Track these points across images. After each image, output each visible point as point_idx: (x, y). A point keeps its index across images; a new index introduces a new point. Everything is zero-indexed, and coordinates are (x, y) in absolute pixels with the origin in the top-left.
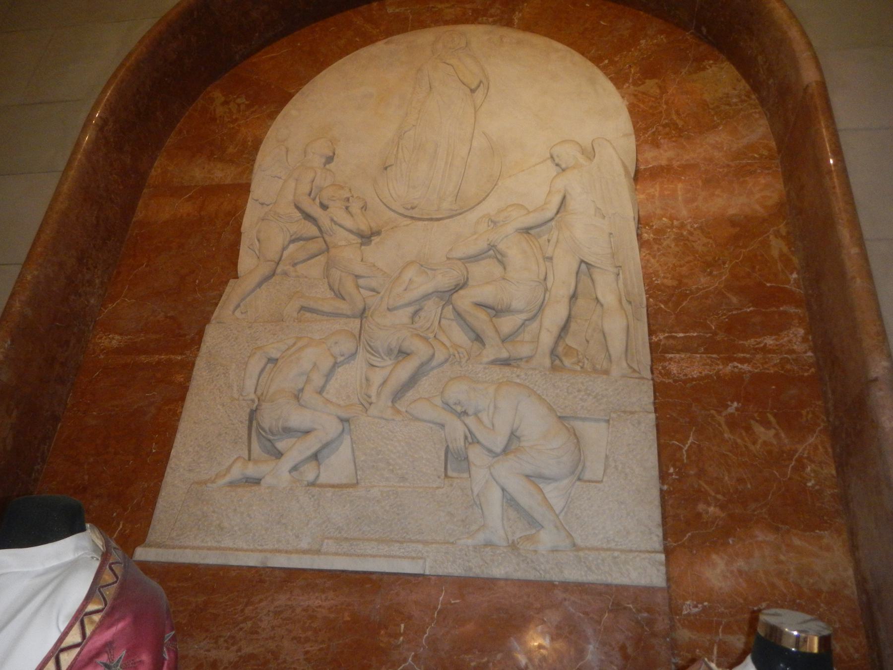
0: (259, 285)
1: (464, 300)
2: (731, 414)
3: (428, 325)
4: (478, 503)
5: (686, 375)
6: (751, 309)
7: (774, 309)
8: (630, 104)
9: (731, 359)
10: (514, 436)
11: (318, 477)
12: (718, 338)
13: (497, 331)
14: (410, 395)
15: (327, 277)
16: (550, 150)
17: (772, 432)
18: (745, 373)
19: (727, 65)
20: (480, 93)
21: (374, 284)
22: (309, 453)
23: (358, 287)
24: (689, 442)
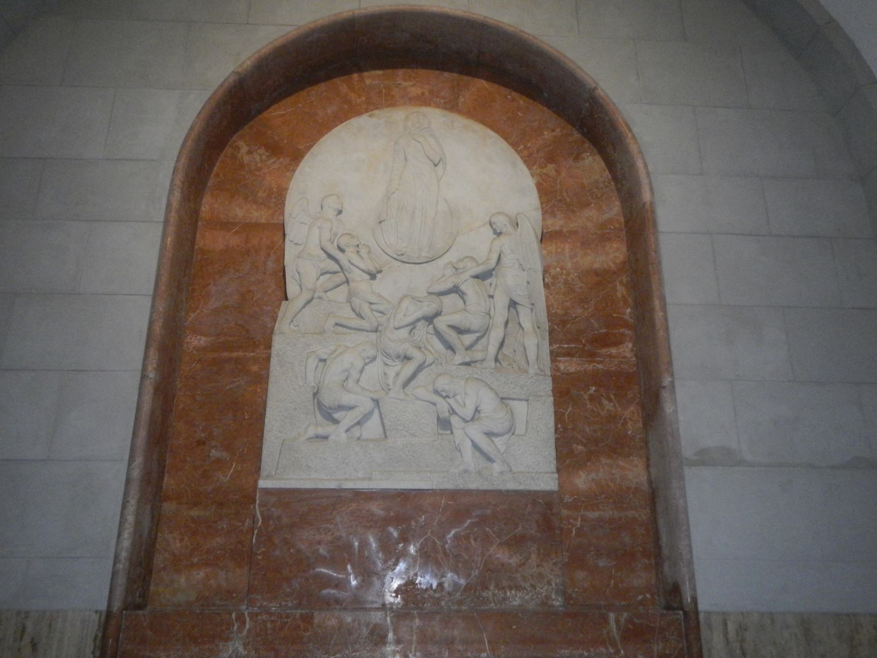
0: (304, 307)
1: (441, 323)
2: (591, 395)
3: (419, 339)
4: (458, 449)
5: (568, 370)
6: (605, 330)
7: (617, 331)
8: (537, 182)
9: (592, 361)
10: (477, 410)
11: (361, 435)
12: (586, 348)
13: (463, 345)
14: (413, 383)
15: (350, 302)
16: (491, 217)
17: (612, 404)
18: (599, 370)
19: (598, 157)
20: (440, 166)
21: (382, 308)
22: (356, 421)
23: (372, 310)
24: (569, 410)
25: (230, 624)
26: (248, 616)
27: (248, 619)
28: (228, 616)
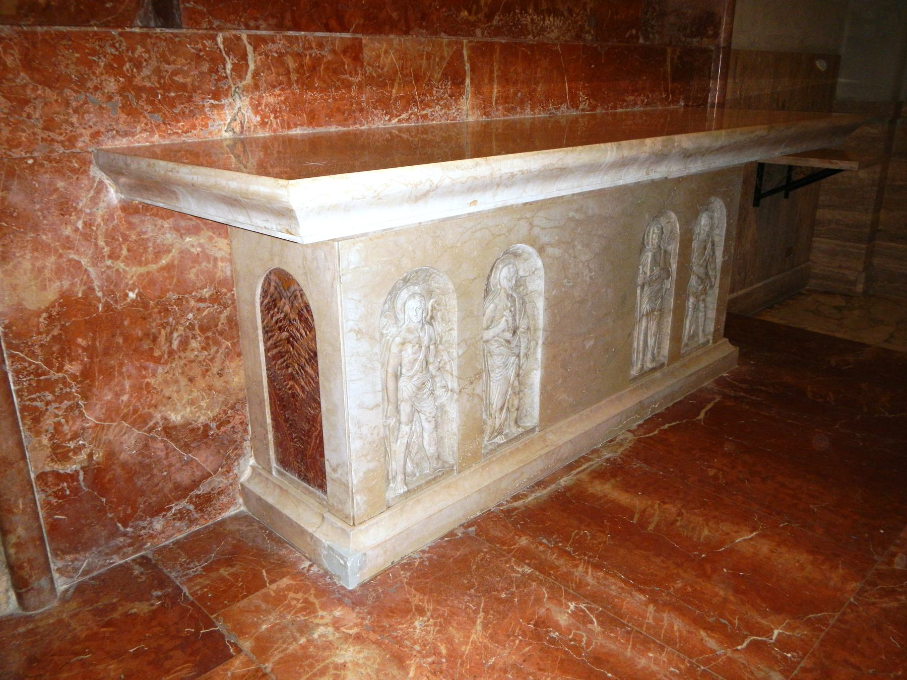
25: (216, 61)
26: (250, 44)
27: (249, 49)
28: (208, 43)
